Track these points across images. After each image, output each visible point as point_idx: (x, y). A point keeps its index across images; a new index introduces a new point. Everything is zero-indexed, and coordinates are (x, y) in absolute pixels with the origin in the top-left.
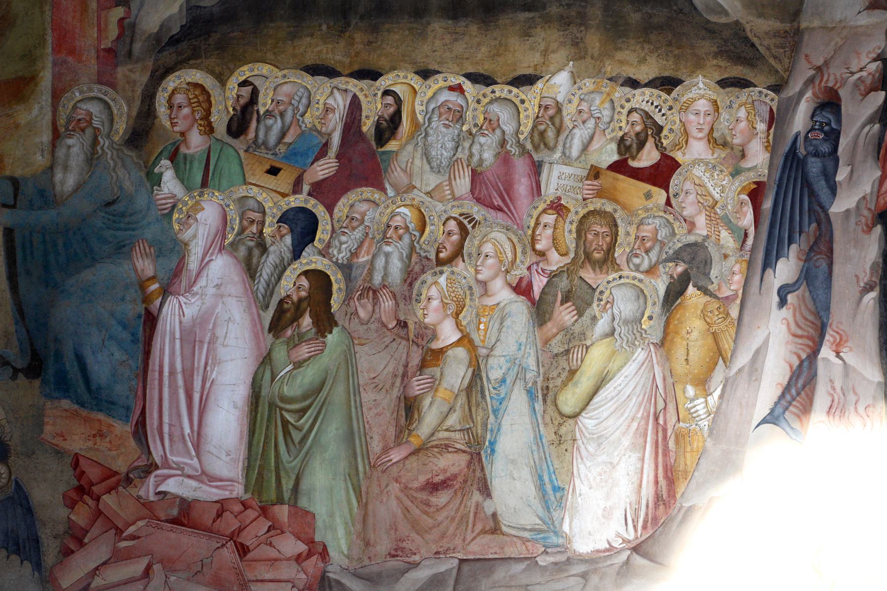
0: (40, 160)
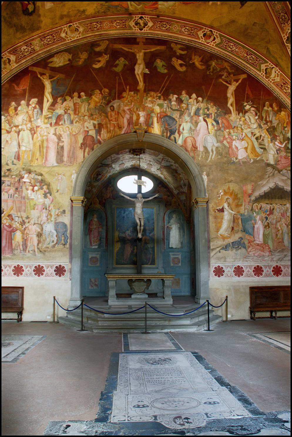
0: (243, 212)
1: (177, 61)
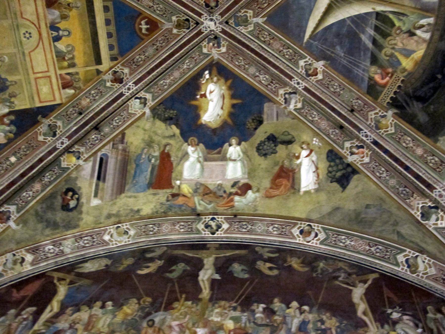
1: (264, 264)
